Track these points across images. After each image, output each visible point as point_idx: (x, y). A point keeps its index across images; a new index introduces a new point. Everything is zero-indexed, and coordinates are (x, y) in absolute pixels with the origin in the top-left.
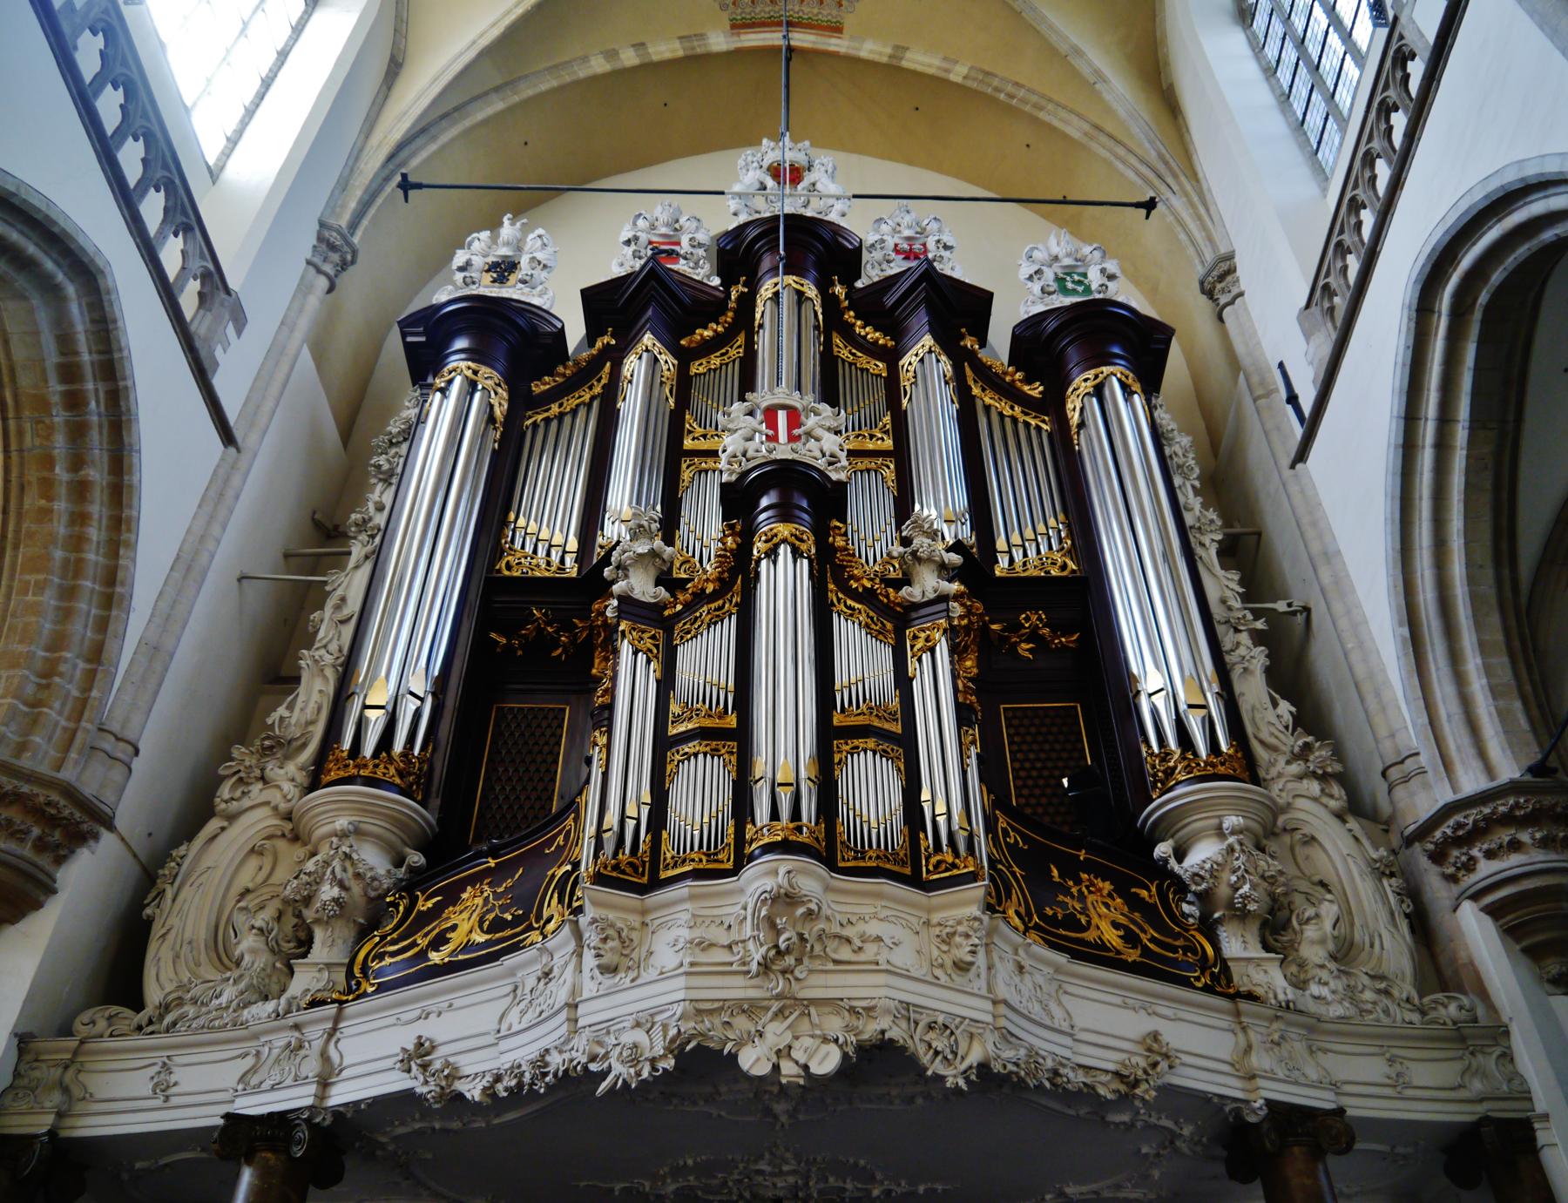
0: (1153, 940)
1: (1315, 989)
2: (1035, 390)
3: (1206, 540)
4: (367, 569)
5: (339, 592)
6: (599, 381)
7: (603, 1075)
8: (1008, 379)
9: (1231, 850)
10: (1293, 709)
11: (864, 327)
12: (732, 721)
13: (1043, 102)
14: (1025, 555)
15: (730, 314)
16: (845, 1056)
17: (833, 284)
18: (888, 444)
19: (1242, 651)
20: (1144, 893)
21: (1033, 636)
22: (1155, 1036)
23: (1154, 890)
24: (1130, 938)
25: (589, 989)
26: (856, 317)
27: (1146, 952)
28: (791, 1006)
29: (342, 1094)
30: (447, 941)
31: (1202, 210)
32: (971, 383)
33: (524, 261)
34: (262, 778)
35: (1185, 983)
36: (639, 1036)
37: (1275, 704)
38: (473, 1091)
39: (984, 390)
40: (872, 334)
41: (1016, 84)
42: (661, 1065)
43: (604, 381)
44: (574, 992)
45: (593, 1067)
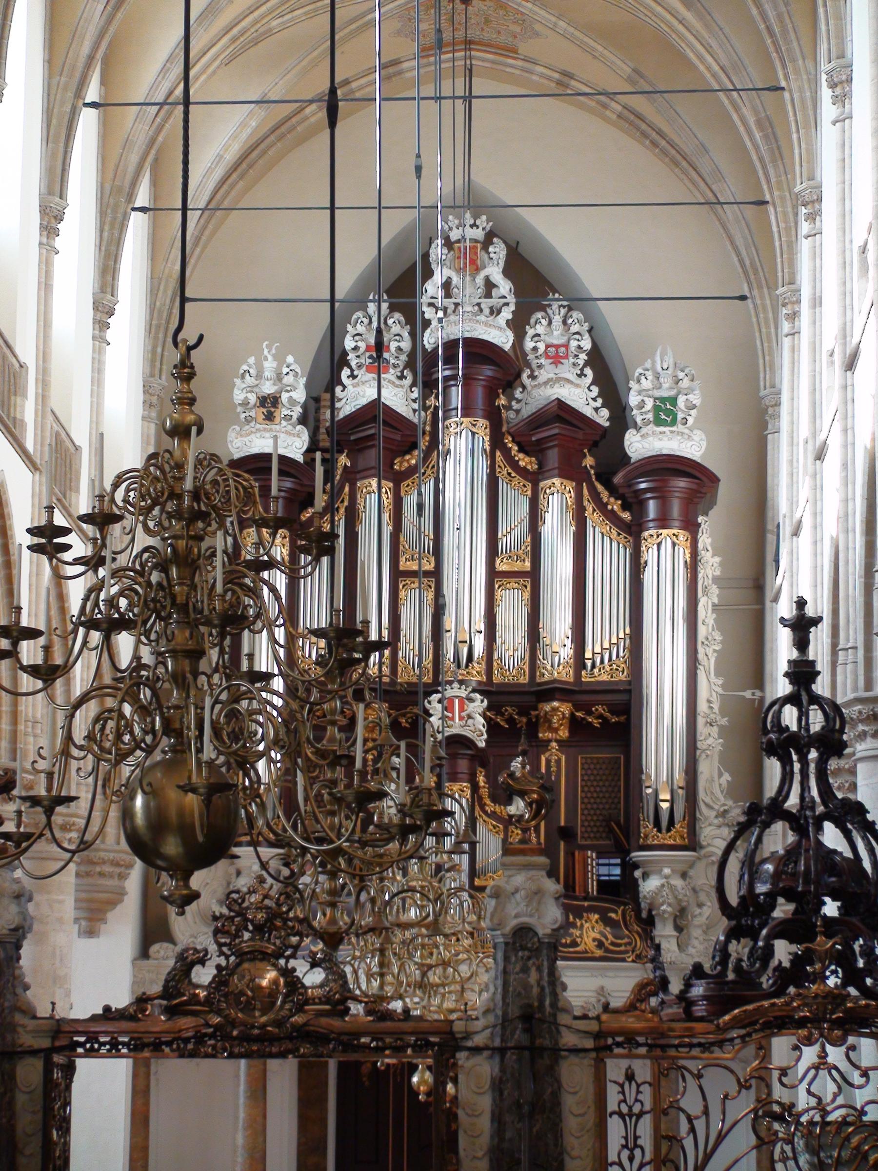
0: (613, 944)
1: (691, 950)
2: (626, 516)
3: (710, 651)
6: (342, 501)
8: (610, 507)
9: (663, 886)
10: (729, 779)
11: (519, 451)
14: (602, 662)
17: (498, 396)
18: (528, 565)
19: (710, 741)
20: (613, 915)
21: (601, 716)
22: (602, 988)
23: (620, 912)
24: (600, 945)
26: (513, 441)
27: (607, 950)
31: (773, 330)
32: (586, 503)
33: (284, 397)
35: (624, 960)
37: (720, 775)
39: (594, 510)
40: (524, 460)
43: (346, 503)
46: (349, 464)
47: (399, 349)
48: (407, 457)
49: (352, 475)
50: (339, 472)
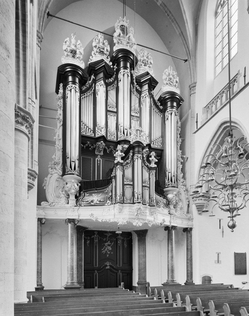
4: (61, 128)
5: (58, 134)
6: (93, 88)
7: (118, 223)
12: (132, 183)
13: (174, 20)
15: (115, 75)
16: (143, 224)
25: (116, 214)
28: (138, 219)
29: (81, 218)
30: (93, 202)
34: (55, 168)
36: (123, 220)
38: (100, 221)
41: (170, 12)
42: (125, 223)
43: (93, 89)
44: (115, 214)
45: (117, 222)
46: (94, 78)
47: (107, 51)
48: (110, 79)
49: (95, 81)
50: (92, 79)
